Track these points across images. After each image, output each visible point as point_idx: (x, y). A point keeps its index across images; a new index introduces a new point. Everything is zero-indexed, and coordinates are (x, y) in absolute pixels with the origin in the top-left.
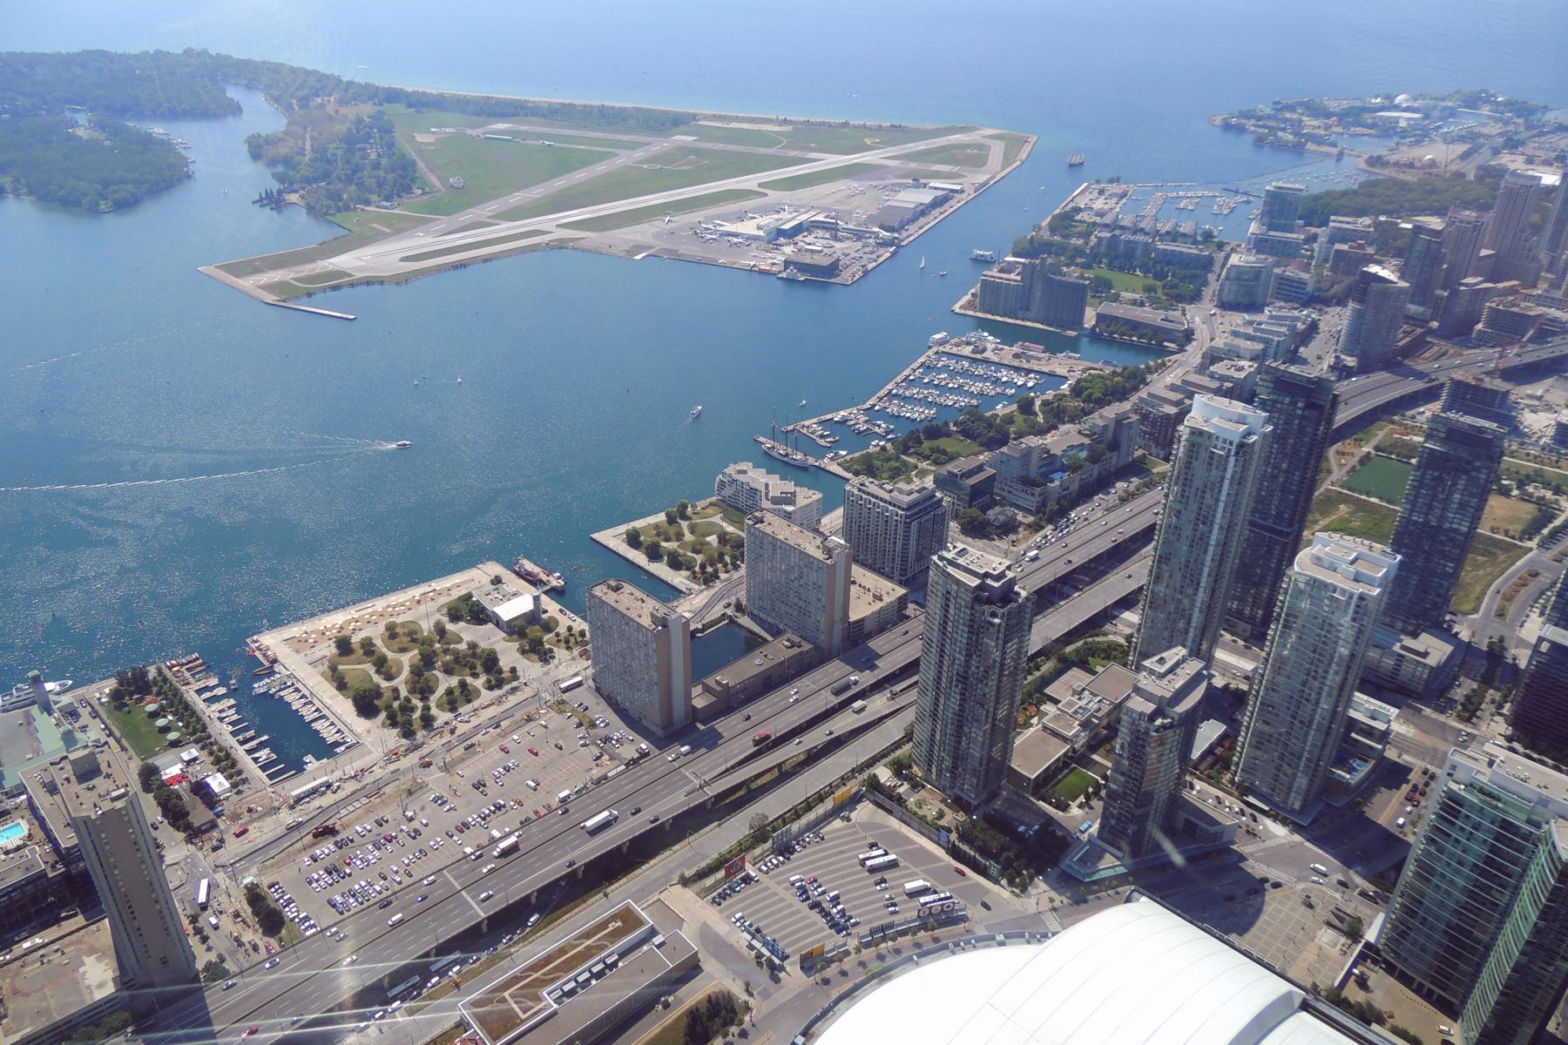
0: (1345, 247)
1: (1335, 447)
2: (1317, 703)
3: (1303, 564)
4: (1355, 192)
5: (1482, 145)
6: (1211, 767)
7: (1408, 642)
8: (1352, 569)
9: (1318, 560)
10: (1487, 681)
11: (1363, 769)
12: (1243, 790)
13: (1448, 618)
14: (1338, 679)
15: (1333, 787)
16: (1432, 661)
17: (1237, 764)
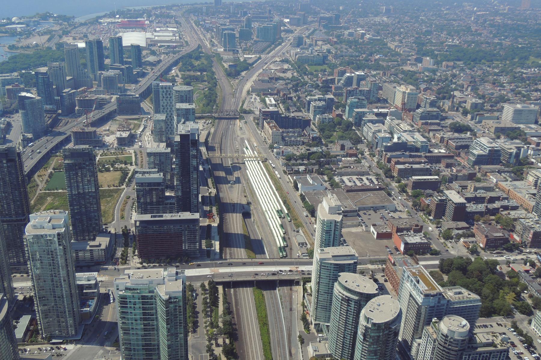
0: (10, 87)
1: (37, 174)
2: (61, 286)
3: (29, 231)
4: (8, 62)
5: (55, 35)
6: (31, 337)
7: (92, 243)
8: (50, 224)
9: (35, 227)
10: (126, 245)
11: (93, 303)
12: (48, 339)
13: (104, 227)
14: (65, 272)
15: (84, 317)
16: (103, 247)
17: (41, 329)
